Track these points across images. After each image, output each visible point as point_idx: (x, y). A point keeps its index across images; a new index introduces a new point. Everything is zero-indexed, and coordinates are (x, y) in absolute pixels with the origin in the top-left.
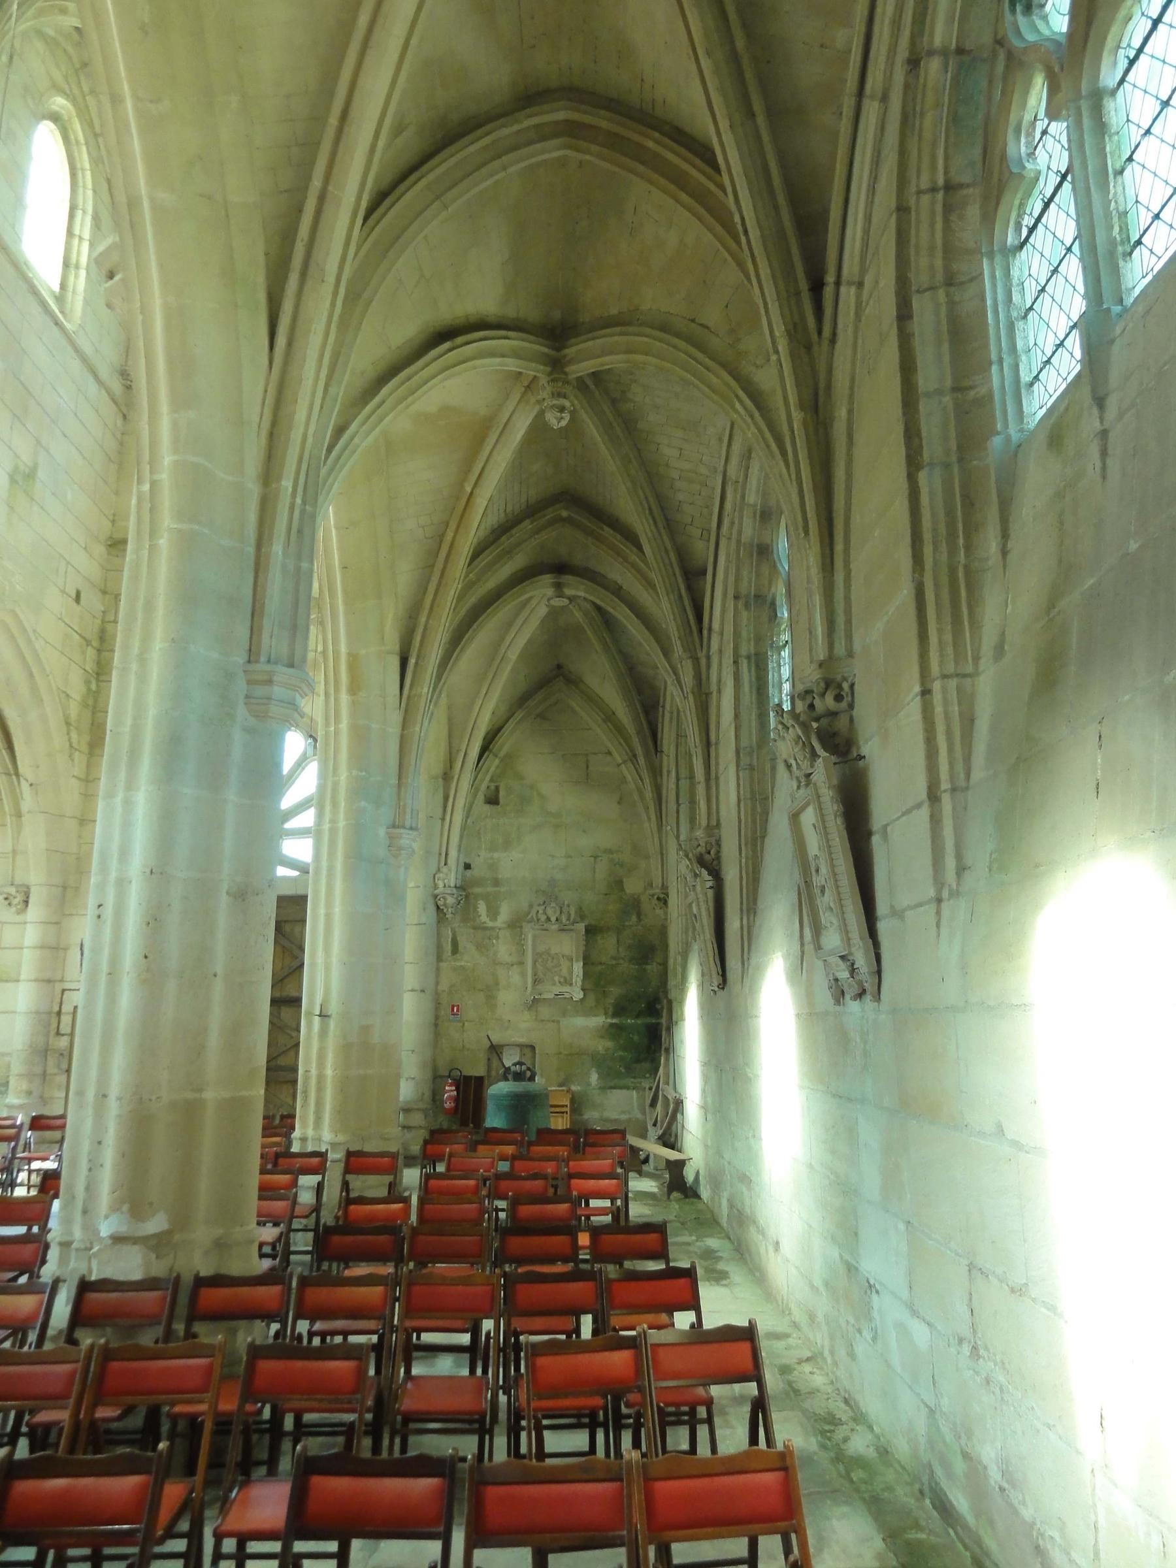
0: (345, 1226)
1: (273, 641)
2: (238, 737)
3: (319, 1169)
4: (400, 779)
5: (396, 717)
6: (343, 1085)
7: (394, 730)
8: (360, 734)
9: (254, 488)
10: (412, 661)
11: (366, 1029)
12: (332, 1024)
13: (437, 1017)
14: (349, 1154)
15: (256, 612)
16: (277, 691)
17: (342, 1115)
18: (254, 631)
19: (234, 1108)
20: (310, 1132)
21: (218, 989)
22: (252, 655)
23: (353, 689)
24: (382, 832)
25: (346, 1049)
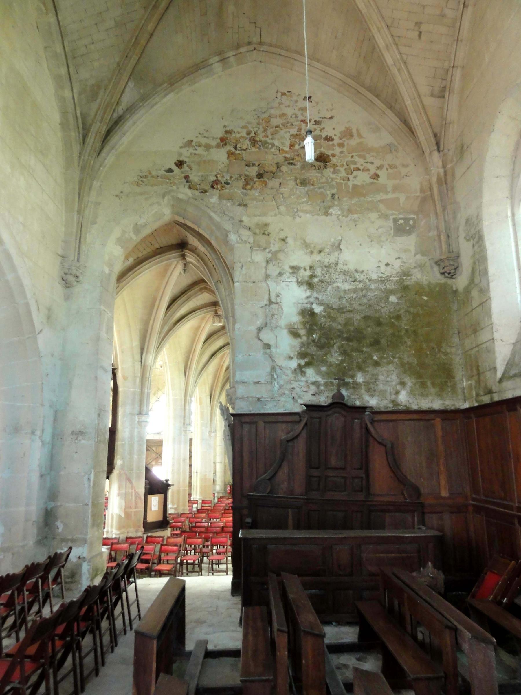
0: (201, 509)
1: (187, 421)
2: (183, 437)
3: (197, 503)
4: (211, 421)
5: (209, 409)
6: (201, 487)
7: (209, 411)
8: (202, 414)
9: (183, 398)
10: (212, 397)
11: (205, 475)
12: (198, 474)
13: (225, 469)
14: (202, 500)
15: (184, 417)
16: (188, 429)
17: (201, 493)
18: (184, 420)
19: (185, 490)
20: (195, 497)
21: (182, 473)
22: (184, 424)
23: (200, 404)
24: (207, 433)
25: (201, 480)
